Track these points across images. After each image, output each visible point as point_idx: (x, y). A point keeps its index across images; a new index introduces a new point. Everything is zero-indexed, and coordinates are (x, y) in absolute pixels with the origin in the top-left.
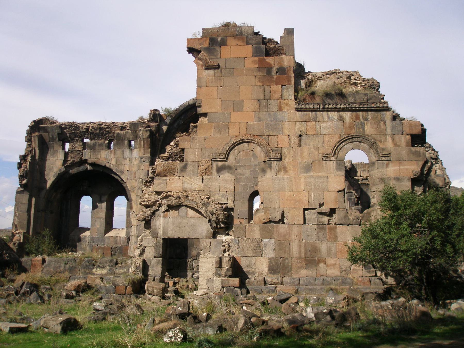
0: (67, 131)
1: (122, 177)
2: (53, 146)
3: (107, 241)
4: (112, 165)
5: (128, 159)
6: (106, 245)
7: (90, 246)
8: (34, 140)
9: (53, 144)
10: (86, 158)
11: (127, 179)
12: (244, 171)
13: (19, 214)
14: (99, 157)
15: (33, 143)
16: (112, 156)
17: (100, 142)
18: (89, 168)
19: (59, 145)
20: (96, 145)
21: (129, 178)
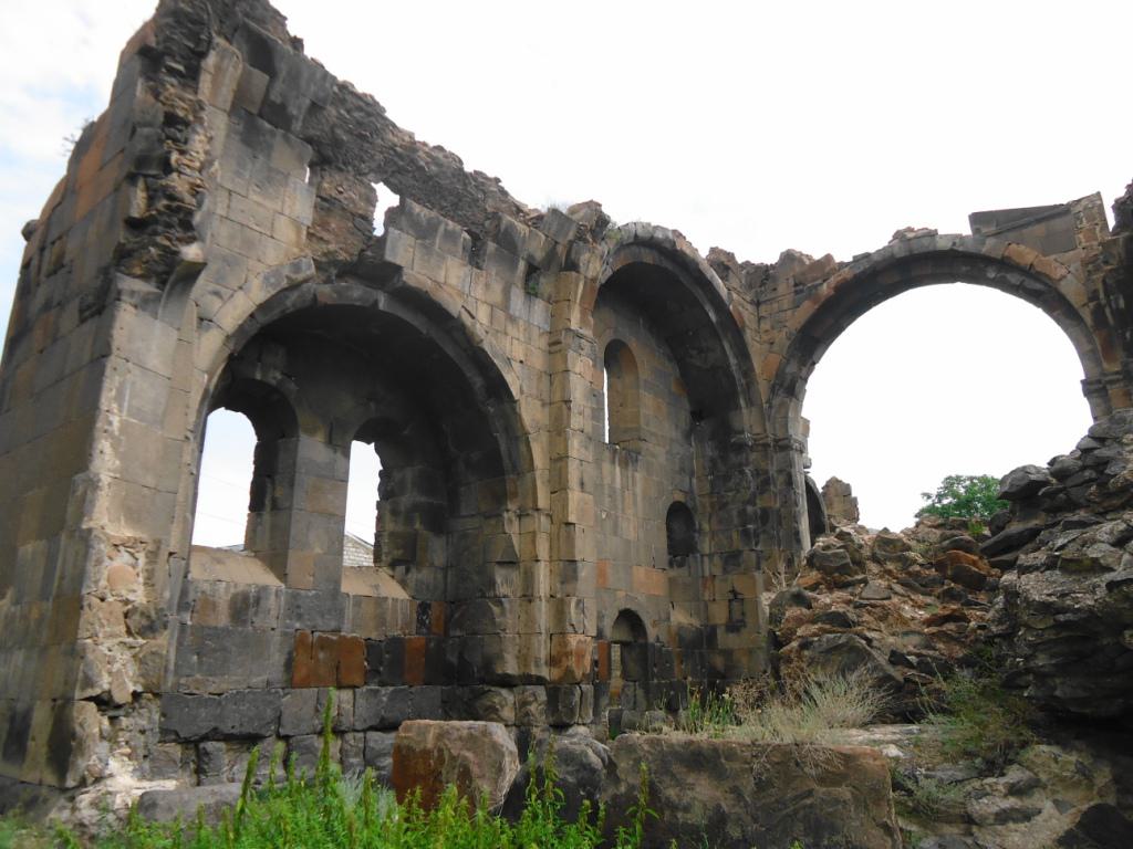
0: (340, 117)
1: (509, 378)
2: (270, 147)
3: (349, 612)
4: (478, 326)
5: (521, 323)
6: (347, 632)
7: (285, 634)
8: (219, 68)
9: (273, 135)
10: (398, 261)
11: (522, 392)
12: (657, 448)
13: (124, 426)
14: (442, 280)
15: (205, 82)
16: (479, 292)
17: (451, 225)
18: (383, 302)
19: (300, 159)
20: (435, 229)
21: (525, 388)
